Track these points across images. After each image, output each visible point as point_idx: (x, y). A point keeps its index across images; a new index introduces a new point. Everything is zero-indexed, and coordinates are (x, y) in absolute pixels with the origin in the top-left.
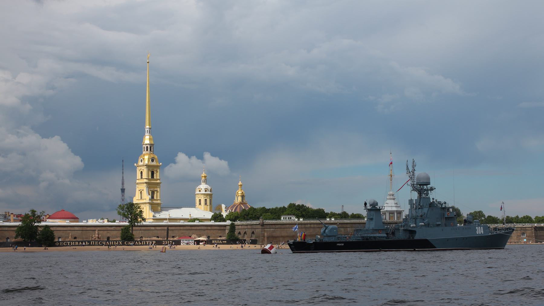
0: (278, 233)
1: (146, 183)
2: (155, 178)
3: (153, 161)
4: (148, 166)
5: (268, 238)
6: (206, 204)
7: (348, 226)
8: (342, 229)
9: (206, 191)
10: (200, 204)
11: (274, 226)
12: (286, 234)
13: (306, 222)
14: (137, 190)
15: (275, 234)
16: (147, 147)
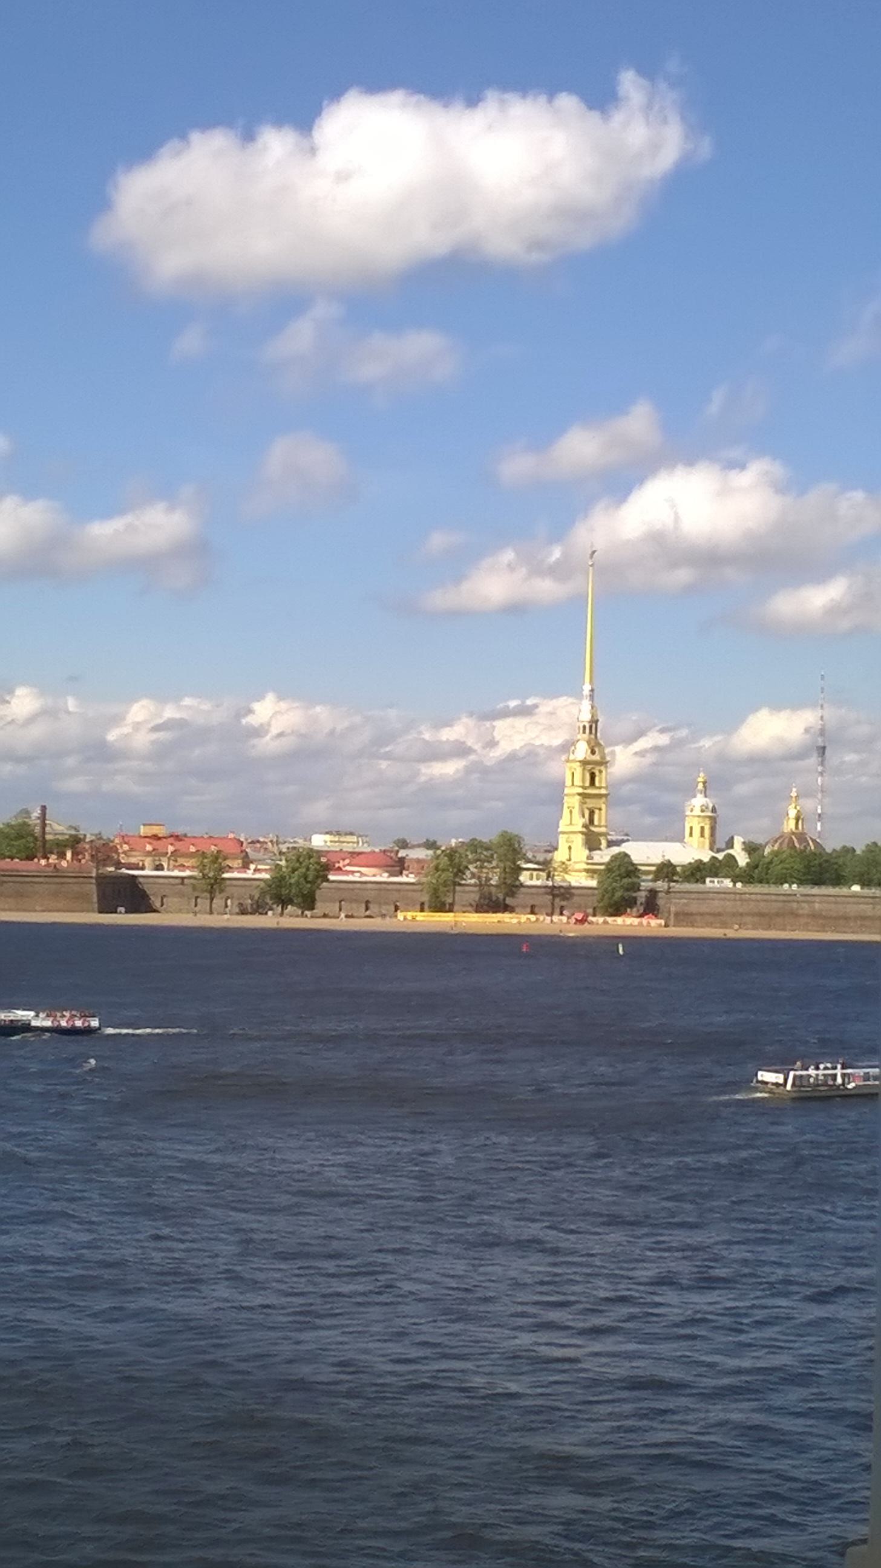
0: (694, 907)
1: (579, 794)
2: (597, 784)
3: (593, 752)
4: (584, 763)
5: (677, 914)
6: (702, 835)
7: (817, 899)
8: (805, 905)
9: (702, 811)
10: (691, 835)
11: (686, 895)
12: (708, 910)
13: (746, 890)
14: (565, 806)
15: (687, 909)
16: (584, 727)
